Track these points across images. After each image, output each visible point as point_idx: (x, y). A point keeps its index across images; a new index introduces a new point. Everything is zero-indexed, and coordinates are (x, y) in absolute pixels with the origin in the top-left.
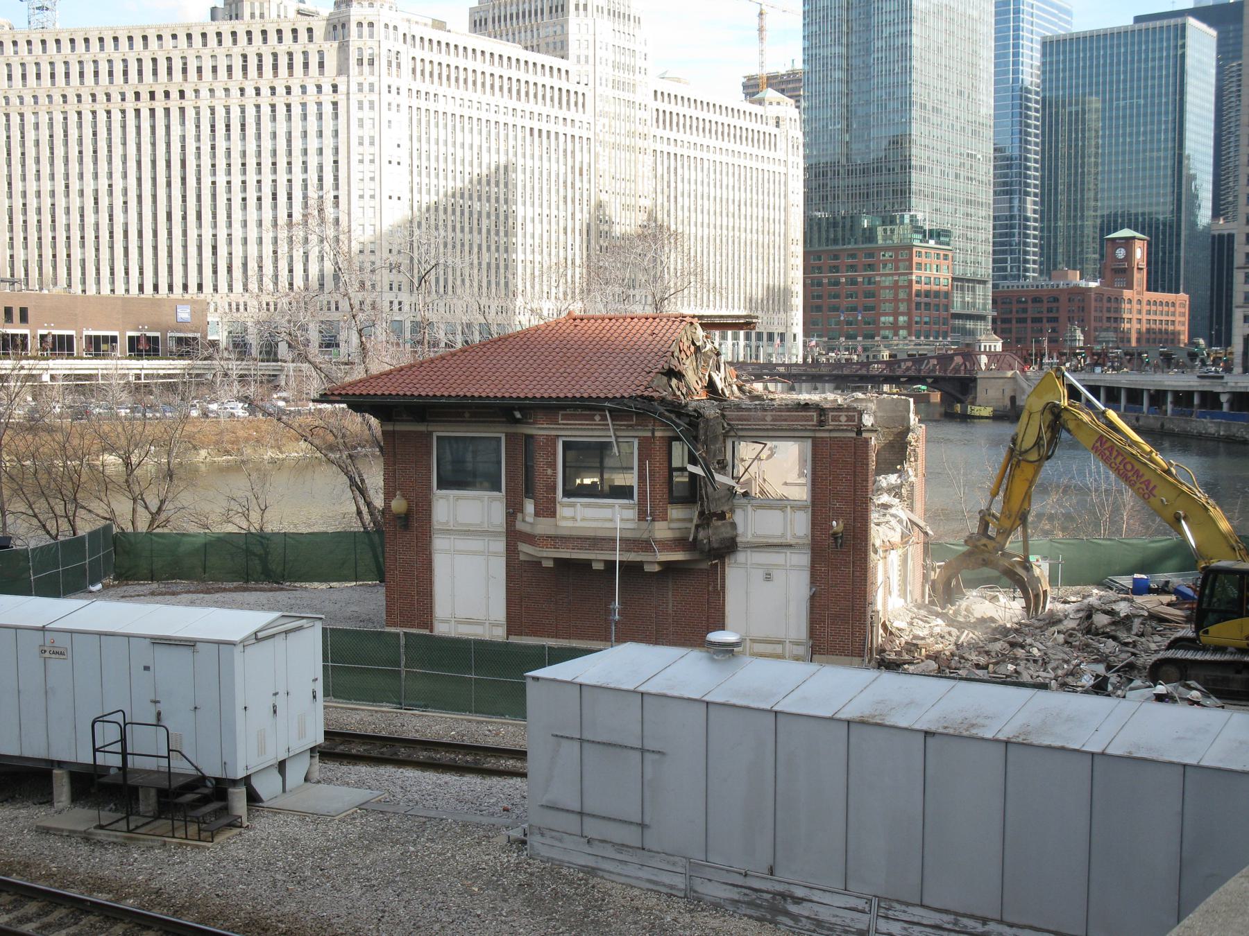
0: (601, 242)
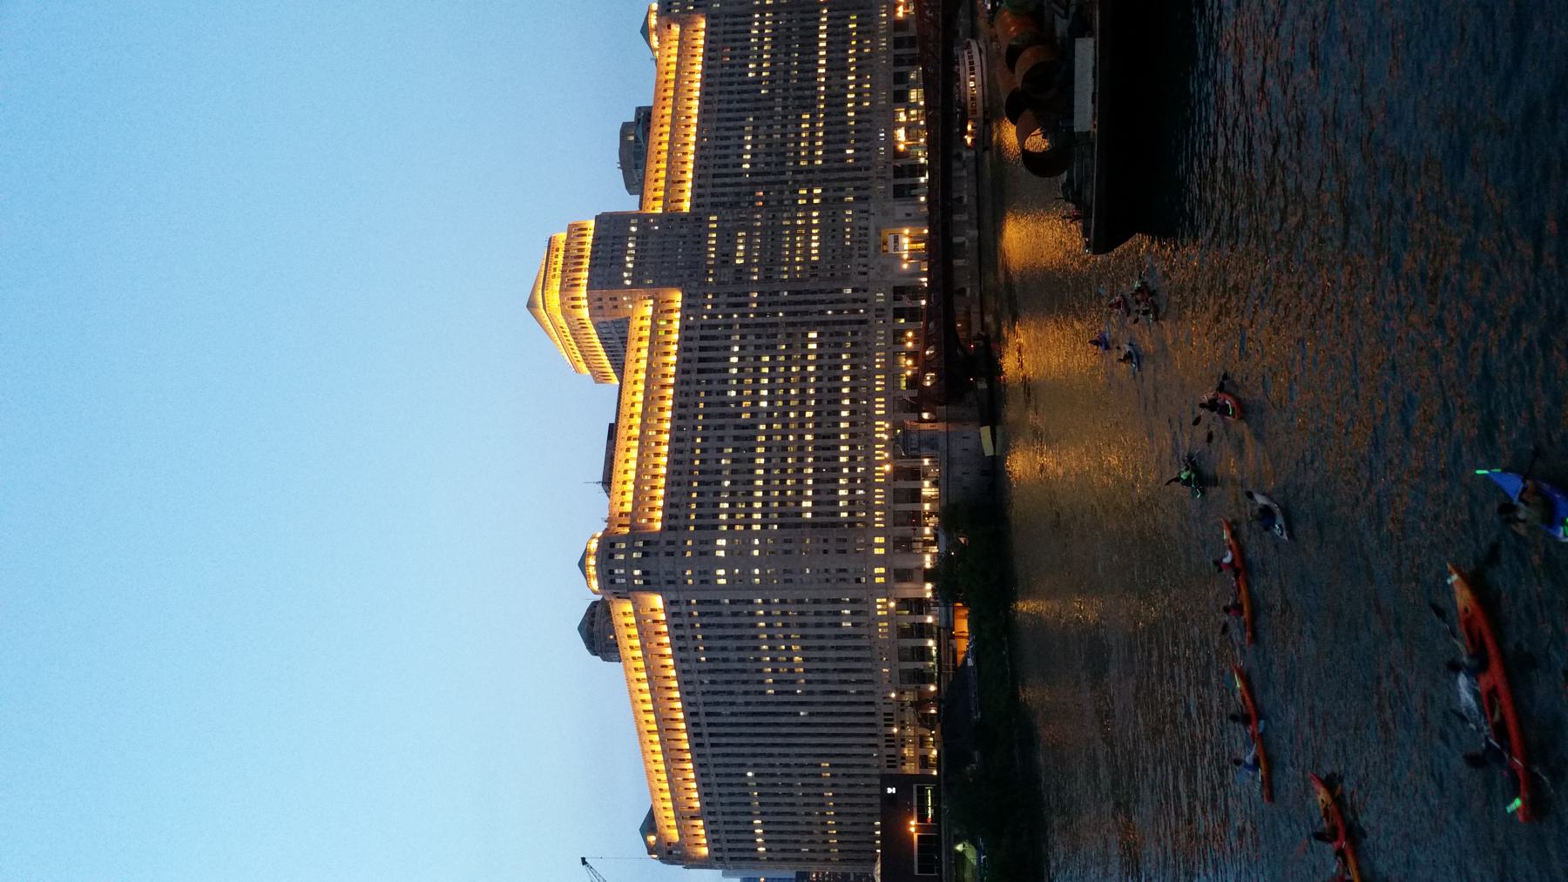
0: (807, 276)
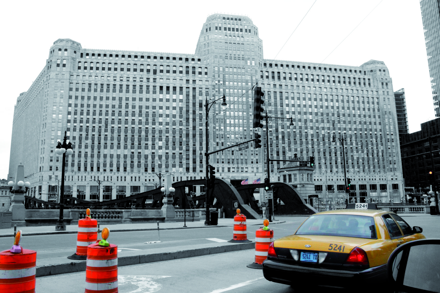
0: (218, 140)
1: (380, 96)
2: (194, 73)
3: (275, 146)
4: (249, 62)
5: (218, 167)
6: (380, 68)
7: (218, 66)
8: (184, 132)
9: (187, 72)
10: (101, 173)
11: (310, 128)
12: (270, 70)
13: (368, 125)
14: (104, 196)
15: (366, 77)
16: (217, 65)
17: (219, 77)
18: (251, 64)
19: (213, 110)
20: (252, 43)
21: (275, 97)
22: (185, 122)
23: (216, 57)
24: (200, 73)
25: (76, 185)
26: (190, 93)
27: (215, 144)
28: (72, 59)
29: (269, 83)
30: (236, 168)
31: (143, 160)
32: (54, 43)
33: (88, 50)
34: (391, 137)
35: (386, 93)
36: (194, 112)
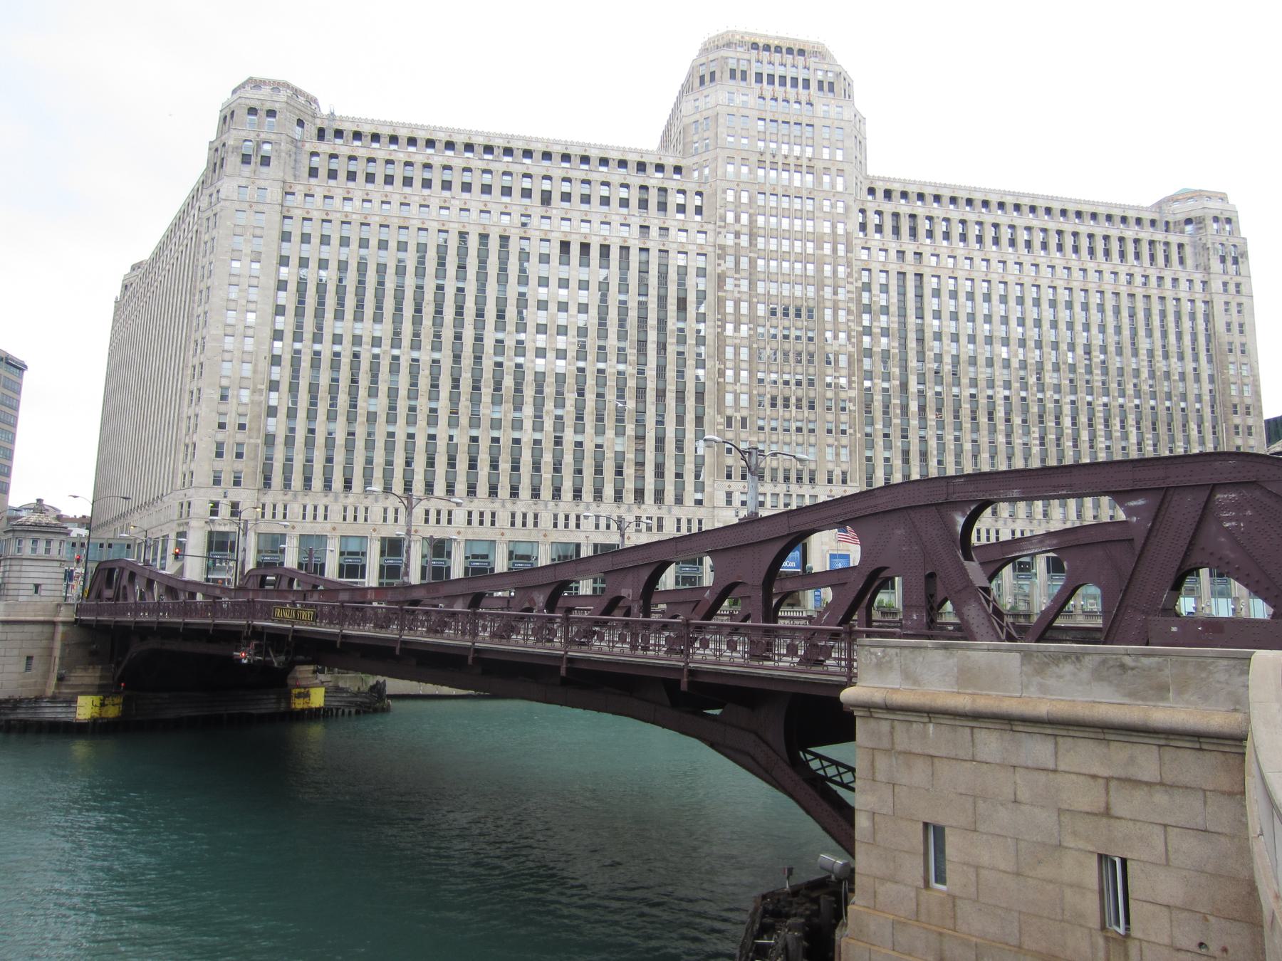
0: (729, 412)
1: (1214, 296)
2: (663, 207)
3: (899, 433)
4: (826, 179)
5: (728, 490)
6: (1217, 213)
7: (736, 188)
8: (631, 383)
9: (643, 204)
10: (376, 501)
11: (1002, 383)
12: (888, 208)
13: (1174, 381)
14: (382, 567)
15: (1174, 239)
16: (733, 185)
17: (737, 219)
18: (833, 185)
19: (719, 320)
20: (837, 124)
21: (902, 290)
22: (635, 351)
23: (731, 160)
24: (681, 208)
25: (298, 532)
26: (651, 266)
27: (722, 420)
28: (292, 142)
29: (885, 247)
30: (782, 496)
31: (507, 462)
32: (234, 92)
33: (342, 119)
34: (1244, 420)
35: (1232, 288)
36: (662, 324)
